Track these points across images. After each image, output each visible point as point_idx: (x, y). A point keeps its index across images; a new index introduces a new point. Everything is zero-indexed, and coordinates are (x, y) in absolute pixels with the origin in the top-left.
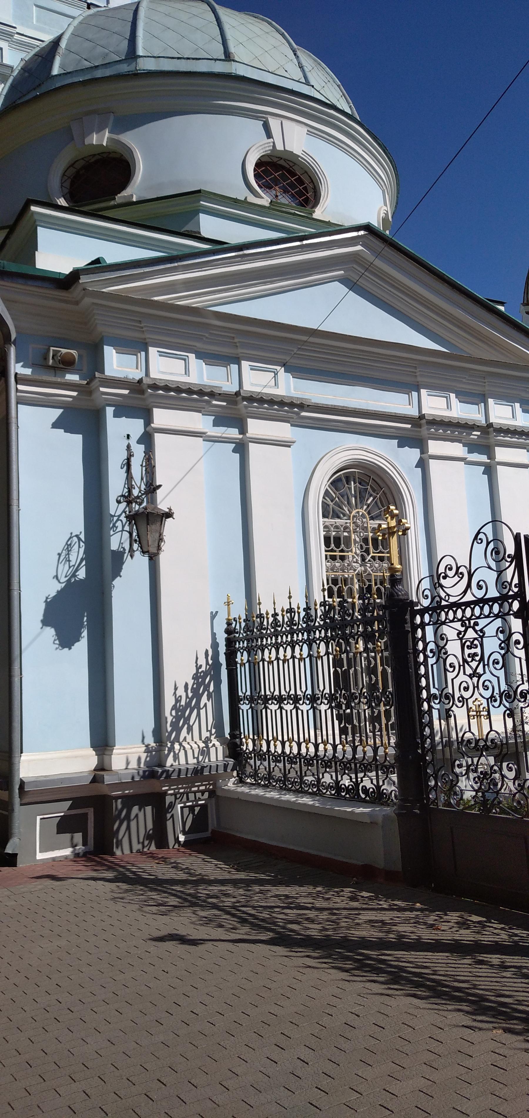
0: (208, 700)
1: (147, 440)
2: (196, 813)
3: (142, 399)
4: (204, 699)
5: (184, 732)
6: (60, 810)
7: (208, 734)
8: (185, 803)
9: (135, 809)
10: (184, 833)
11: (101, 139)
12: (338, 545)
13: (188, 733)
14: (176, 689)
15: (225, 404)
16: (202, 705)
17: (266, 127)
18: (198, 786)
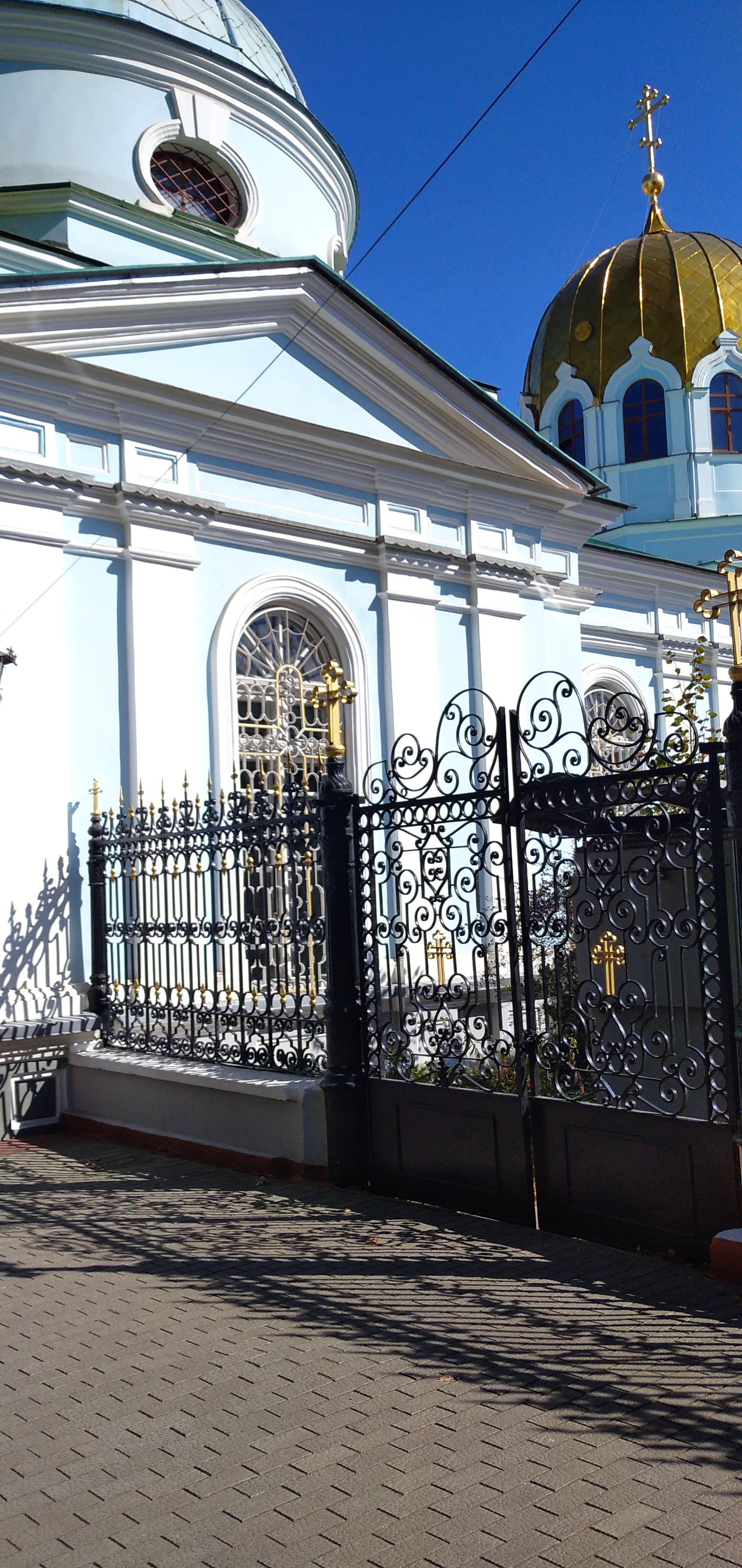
0: (61, 929)
2: (38, 1090)
4: (55, 928)
5: (23, 975)
7: (59, 978)
8: (21, 1076)
10: (19, 1118)
12: (257, 714)
13: (30, 977)
14: (13, 913)
15: (98, 501)
16: (51, 936)
17: (171, 101)
18: (43, 1052)
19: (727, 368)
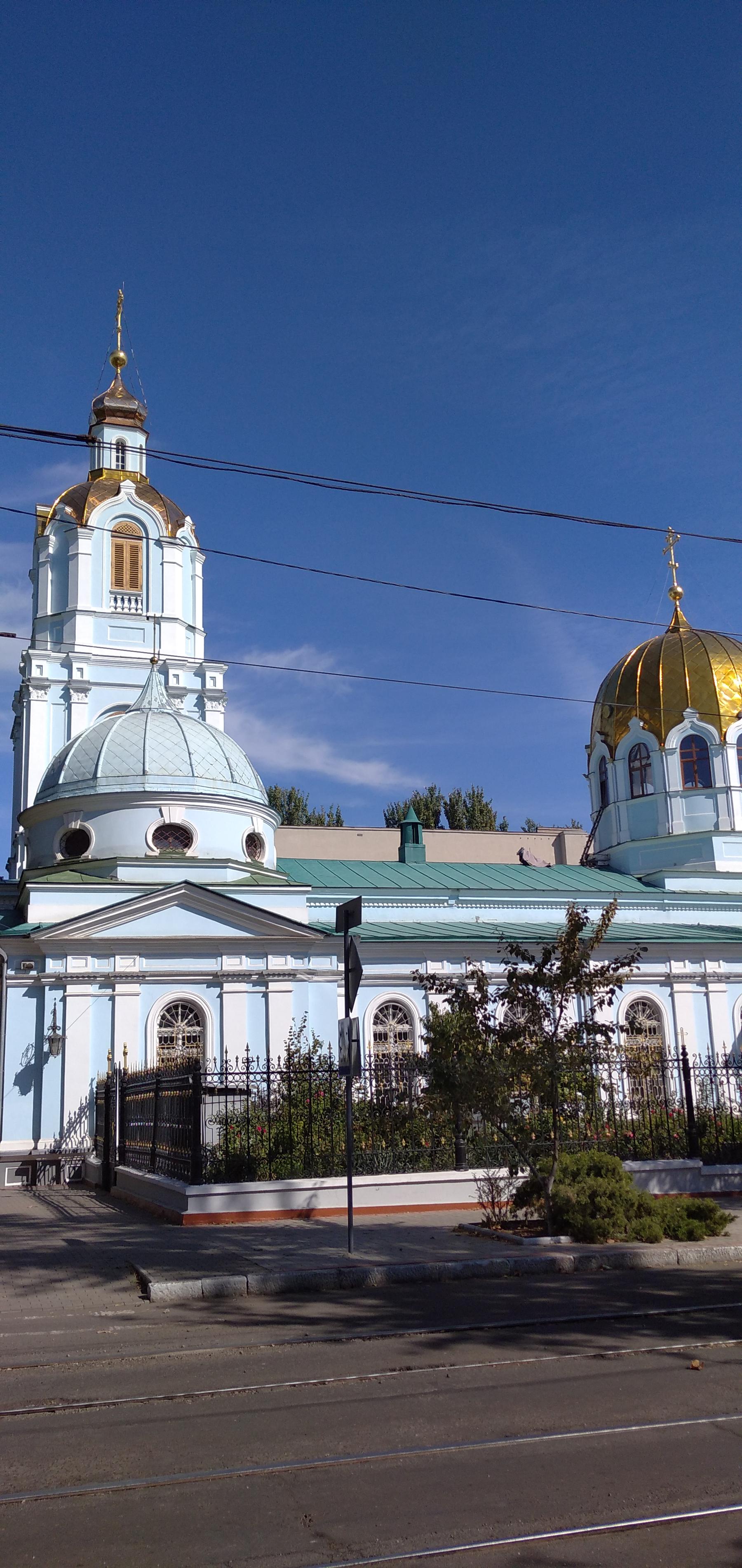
1: (64, 999)
3: (61, 982)
4: (84, 1119)
5: (73, 1134)
6: (17, 1166)
9: (48, 1167)
10: (69, 1178)
11: (76, 825)
12: (166, 1042)
17: (161, 811)
19: (692, 732)
